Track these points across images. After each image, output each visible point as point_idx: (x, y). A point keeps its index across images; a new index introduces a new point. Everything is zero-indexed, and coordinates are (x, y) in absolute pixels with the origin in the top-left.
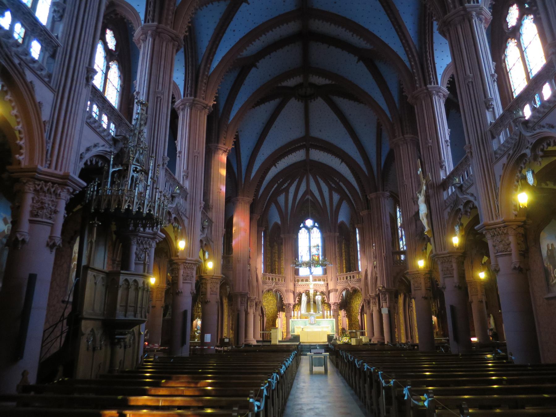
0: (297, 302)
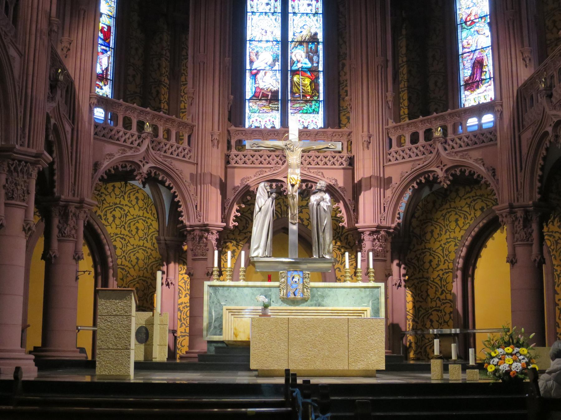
0: (232, 224)
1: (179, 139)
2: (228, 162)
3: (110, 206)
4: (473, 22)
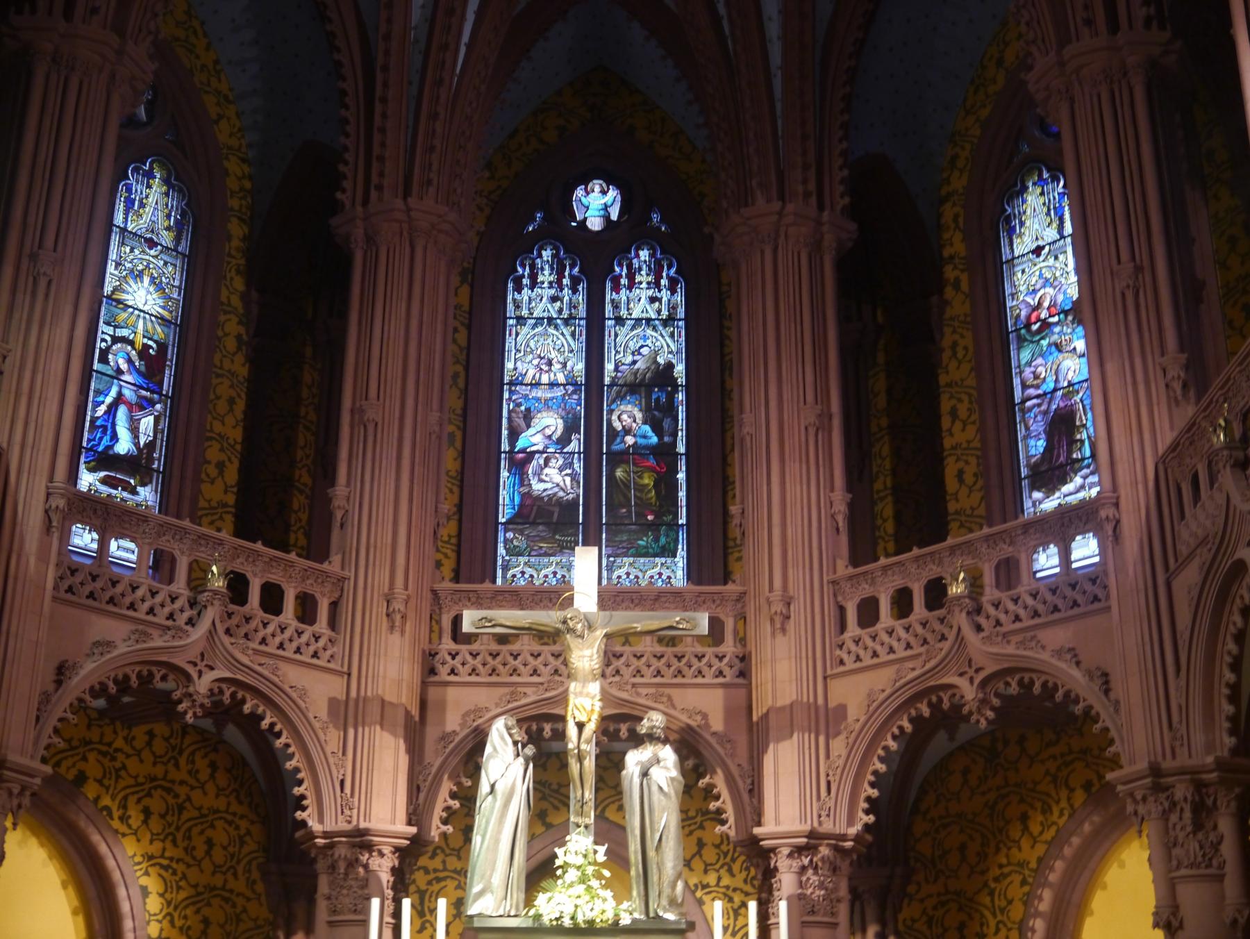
1: (307, 610)
2: (433, 671)
3: (138, 785)
4: (1045, 325)
